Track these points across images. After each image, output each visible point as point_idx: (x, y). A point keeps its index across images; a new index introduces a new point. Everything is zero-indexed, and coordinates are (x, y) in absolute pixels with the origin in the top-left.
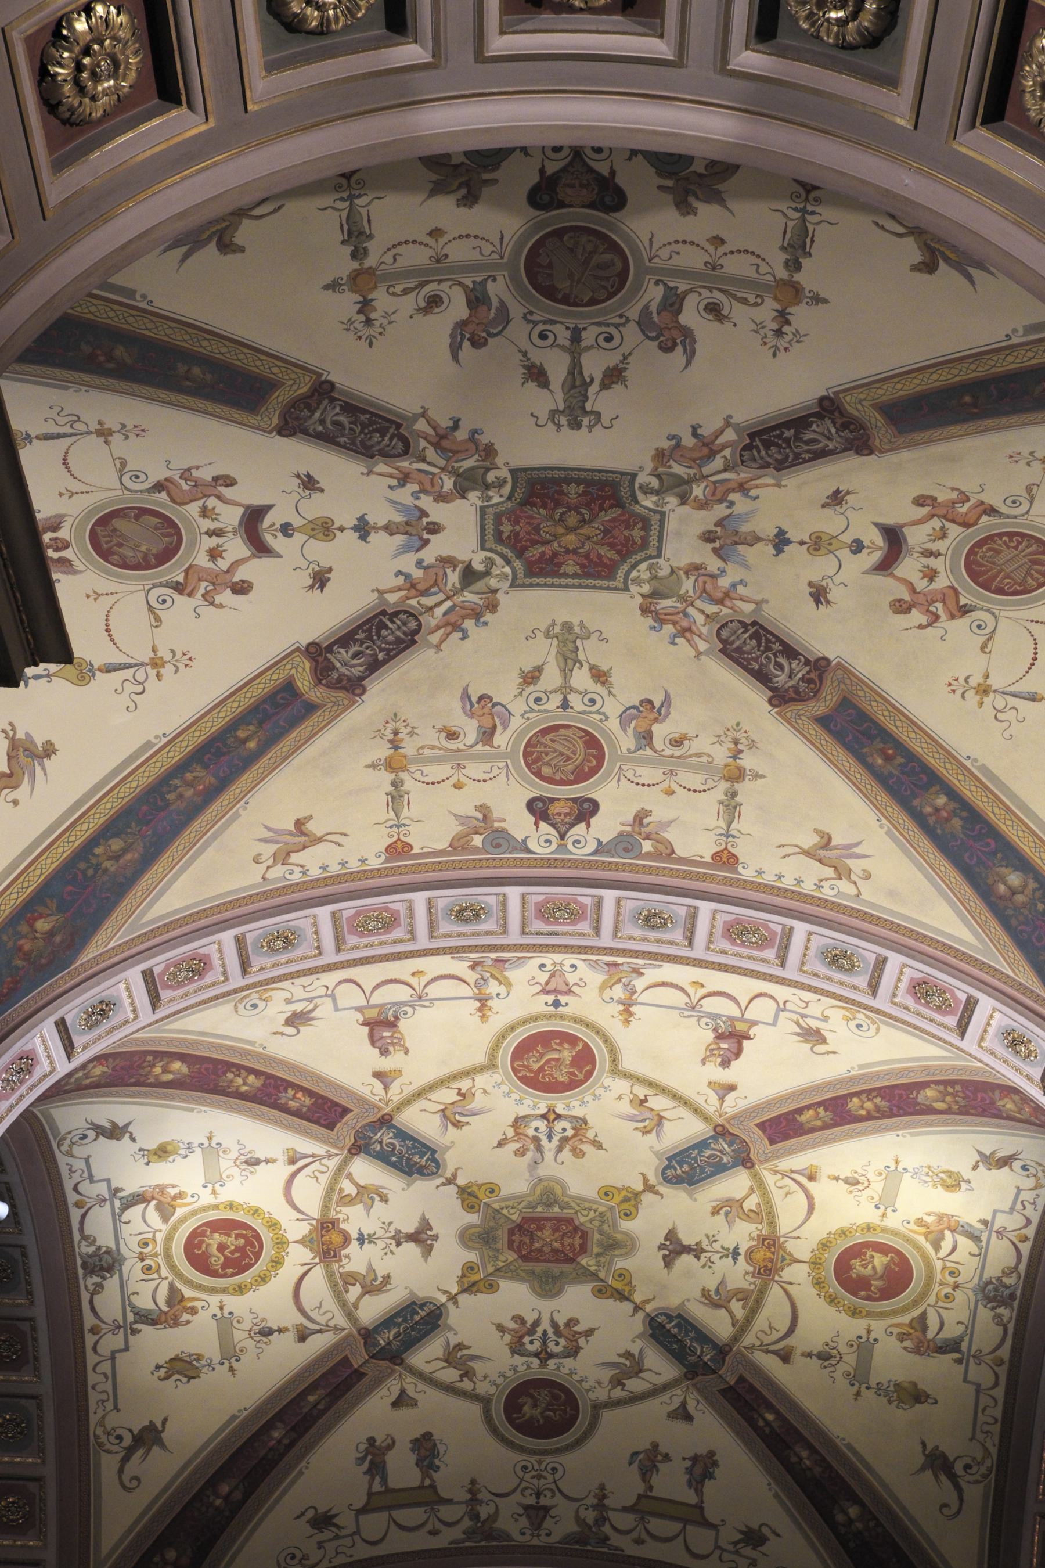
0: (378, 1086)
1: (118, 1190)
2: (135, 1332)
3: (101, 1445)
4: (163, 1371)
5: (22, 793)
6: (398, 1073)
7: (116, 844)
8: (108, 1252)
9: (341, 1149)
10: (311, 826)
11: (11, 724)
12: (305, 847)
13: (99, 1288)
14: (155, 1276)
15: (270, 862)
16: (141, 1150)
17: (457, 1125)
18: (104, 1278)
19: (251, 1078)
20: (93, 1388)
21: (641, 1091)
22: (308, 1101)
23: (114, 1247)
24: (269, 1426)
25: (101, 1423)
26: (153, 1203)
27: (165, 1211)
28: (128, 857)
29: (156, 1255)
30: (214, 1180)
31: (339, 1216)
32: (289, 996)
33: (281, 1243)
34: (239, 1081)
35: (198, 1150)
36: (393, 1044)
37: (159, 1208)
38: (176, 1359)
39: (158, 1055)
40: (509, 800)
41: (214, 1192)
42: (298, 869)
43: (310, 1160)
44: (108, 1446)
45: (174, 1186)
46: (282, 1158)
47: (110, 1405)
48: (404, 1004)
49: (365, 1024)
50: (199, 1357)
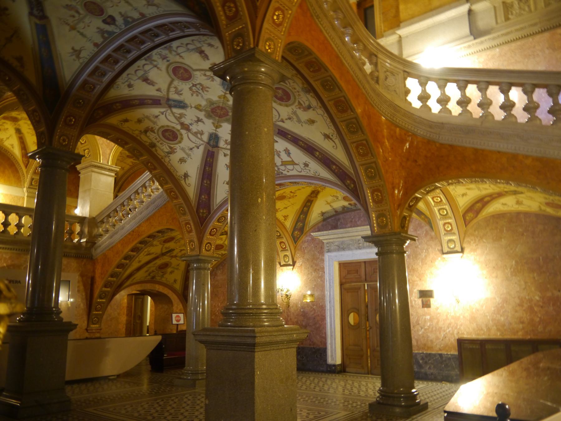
13: (156, 151)
17: (181, 94)
21: (203, 72)
24: (205, 168)
27: (153, 131)
38: (180, 159)
40: (97, 22)
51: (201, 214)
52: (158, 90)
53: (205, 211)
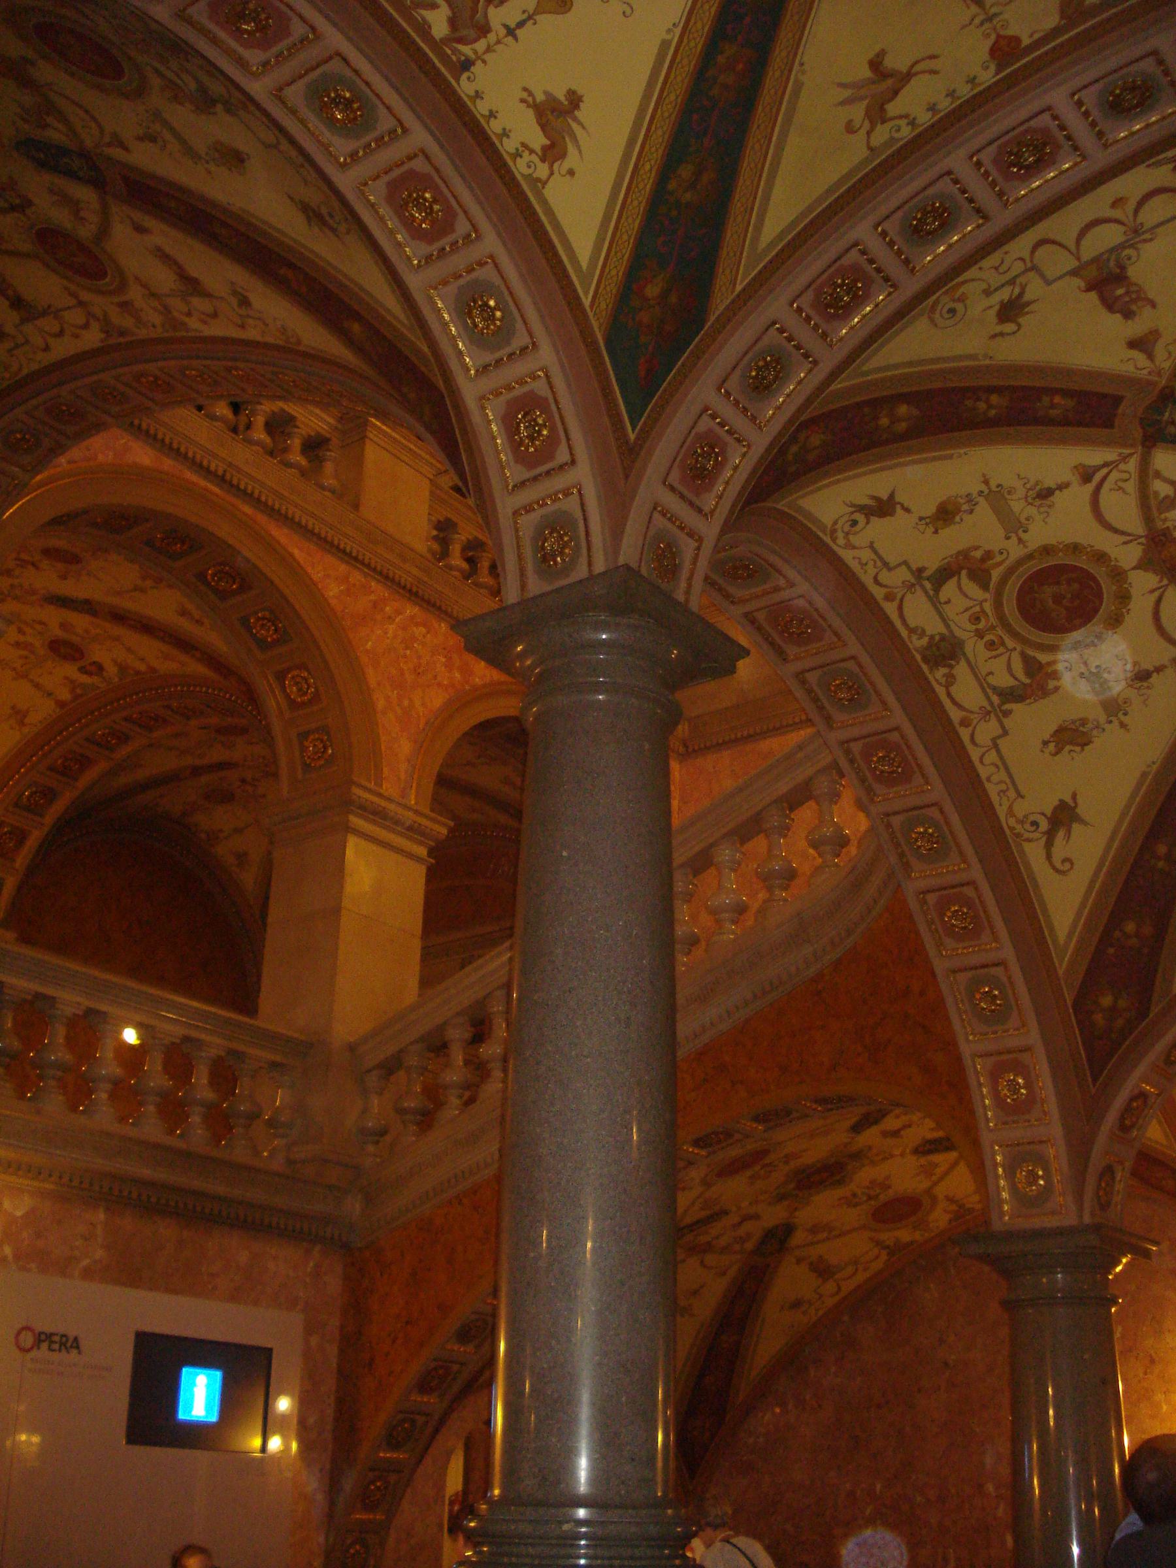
0: (1140, 357)
1: (921, 570)
2: (1007, 713)
3: (1018, 835)
4: (1052, 746)
5: (572, 159)
6: (1155, 334)
7: (686, 171)
8: (943, 638)
9: (1132, 446)
10: (889, 63)
11: (525, 89)
12: (896, 93)
13: (950, 680)
14: (1002, 650)
15: (867, 124)
16: (921, 519)
18: (951, 667)
19: (994, 399)
20: (988, 779)
22: (1070, 403)
23: (944, 631)
25: (1010, 812)
26: (964, 572)
28: (705, 179)
29: (993, 628)
30: (1014, 526)
31: (1169, 524)
32: (984, 286)
33: (1118, 575)
34: (982, 406)
35: (981, 500)
36: (1133, 301)
37: (973, 576)
38: (1060, 731)
39: (875, 403)
41: (1020, 540)
42: (903, 122)
43: (1105, 471)
44: (1026, 835)
45: (976, 548)
46: (1075, 479)
47: (1012, 794)
48: (1122, 246)
49: (1089, 289)
50: (1084, 722)
51: (1099, 1018)
52: (1142, 344)
53: (1122, 1003)
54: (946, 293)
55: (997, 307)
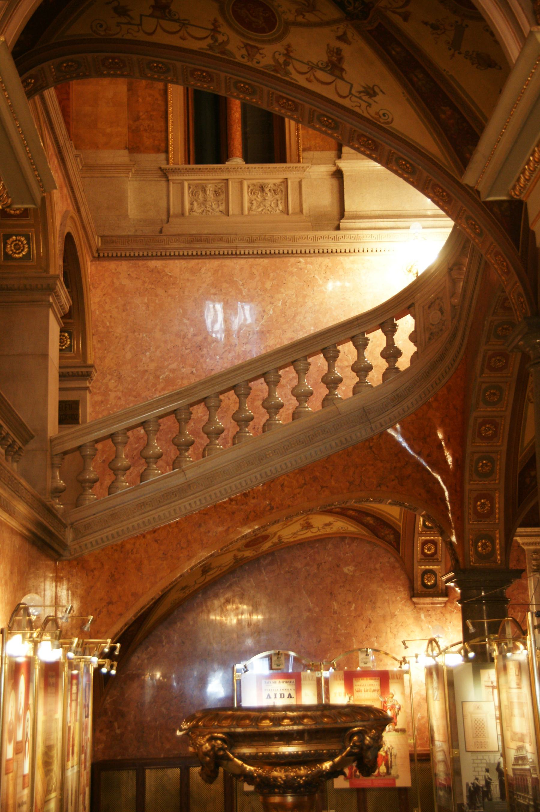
54: (379, 122)
55: (373, 98)
